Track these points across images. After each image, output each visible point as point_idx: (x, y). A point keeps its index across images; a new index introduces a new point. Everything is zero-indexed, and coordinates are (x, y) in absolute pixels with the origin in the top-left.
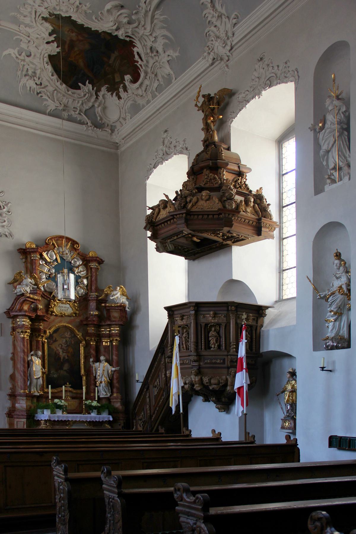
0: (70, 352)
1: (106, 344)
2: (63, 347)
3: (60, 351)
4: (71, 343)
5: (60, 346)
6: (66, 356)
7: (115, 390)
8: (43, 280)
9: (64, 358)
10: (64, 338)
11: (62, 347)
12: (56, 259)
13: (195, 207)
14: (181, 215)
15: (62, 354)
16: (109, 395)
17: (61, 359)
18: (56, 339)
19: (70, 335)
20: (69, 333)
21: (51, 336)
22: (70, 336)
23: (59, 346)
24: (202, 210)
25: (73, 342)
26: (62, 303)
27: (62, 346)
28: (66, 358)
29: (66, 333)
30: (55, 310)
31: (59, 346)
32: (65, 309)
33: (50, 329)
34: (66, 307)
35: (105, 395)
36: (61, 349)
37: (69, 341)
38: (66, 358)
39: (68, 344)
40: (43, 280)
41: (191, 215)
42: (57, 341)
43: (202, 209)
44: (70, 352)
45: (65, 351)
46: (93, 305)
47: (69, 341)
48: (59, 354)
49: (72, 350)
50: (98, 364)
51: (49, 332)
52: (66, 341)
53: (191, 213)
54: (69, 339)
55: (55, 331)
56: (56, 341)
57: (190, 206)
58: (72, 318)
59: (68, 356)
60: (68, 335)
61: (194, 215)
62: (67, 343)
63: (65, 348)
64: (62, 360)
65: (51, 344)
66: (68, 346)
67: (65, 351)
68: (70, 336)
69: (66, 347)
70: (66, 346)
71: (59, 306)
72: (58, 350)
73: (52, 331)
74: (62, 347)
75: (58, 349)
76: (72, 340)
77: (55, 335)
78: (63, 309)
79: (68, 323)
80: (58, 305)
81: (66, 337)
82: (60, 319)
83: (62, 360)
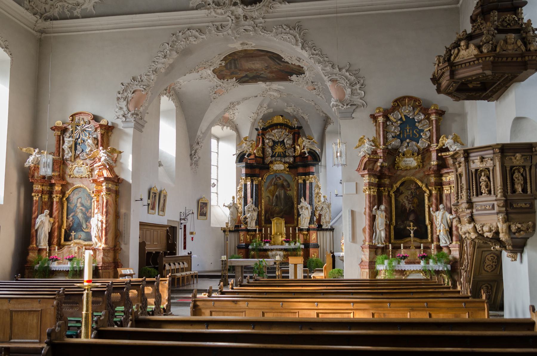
0: (416, 202)
1: (447, 192)
2: (409, 198)
3: (406, 202)
4: (416, 194)
5: (406, 197)
6: (412, 207)
7: (454, 238)
8: (390, 139)
9: (410, 209)
10: (409, 190)
11: (407, 199)
12: (401, 118)
13: (458, 58)
14: (446, 68)
15: (408, 206)
16: (448, 243)
17: (407, 209)
18: (402, 191)
19: (415, 186)
20: (414, 184)
21: (398, 189)
22: (415, 187)
23: (405, 198)
24: (463, 59)
25: (418, 193)
26: (407, 158)
27: (408, 197)
28: (412, 209)
29: (411, 185)
30: (400, 165)
31: (405, 198)
32: (409, 162)
33: (396, 183)
34: (410, 161)
35: (445, 243)
36: (407, 200)
37: (414, 192)
38: (412, 209)
39: (413, 195)
40: (390, 139)
41: (455, 66)
42: (403, 193)
43: (463, 58)
44: (416, 202)
45: (411, 203)
46: (434, 155)
47: (414, 192)
48: (405, 206)
49: (417, 200)
50: (438, 212)
51: (396, 186)
52: (412, 192)
53: (454, 65)
54: (414, 190)
55: (402, 184)
56: (402, 193)
57: (452, 57)
58: (417, 170)
59: (413, 207)
60: (413, 187)
61: (458, 65)
62: (412, 194)
63: (411, 200)
64: (408, 211)
65: (398, 197)
66: (413, 197)
67: (411, 203)
68: (415, 187)
69: (412, 198)
70: (411, 197)
71: (404, 161)
72: (404, 202)
73: (398, 184)
74: (407, 199)
75: (405, 200)
76: (417, 191)
77: (401, 188)
78: (408, 162)
79: (414, 175)
80: (403, 160)
81: (412, 189)
82: (406, 171)
83: (408, 211)
